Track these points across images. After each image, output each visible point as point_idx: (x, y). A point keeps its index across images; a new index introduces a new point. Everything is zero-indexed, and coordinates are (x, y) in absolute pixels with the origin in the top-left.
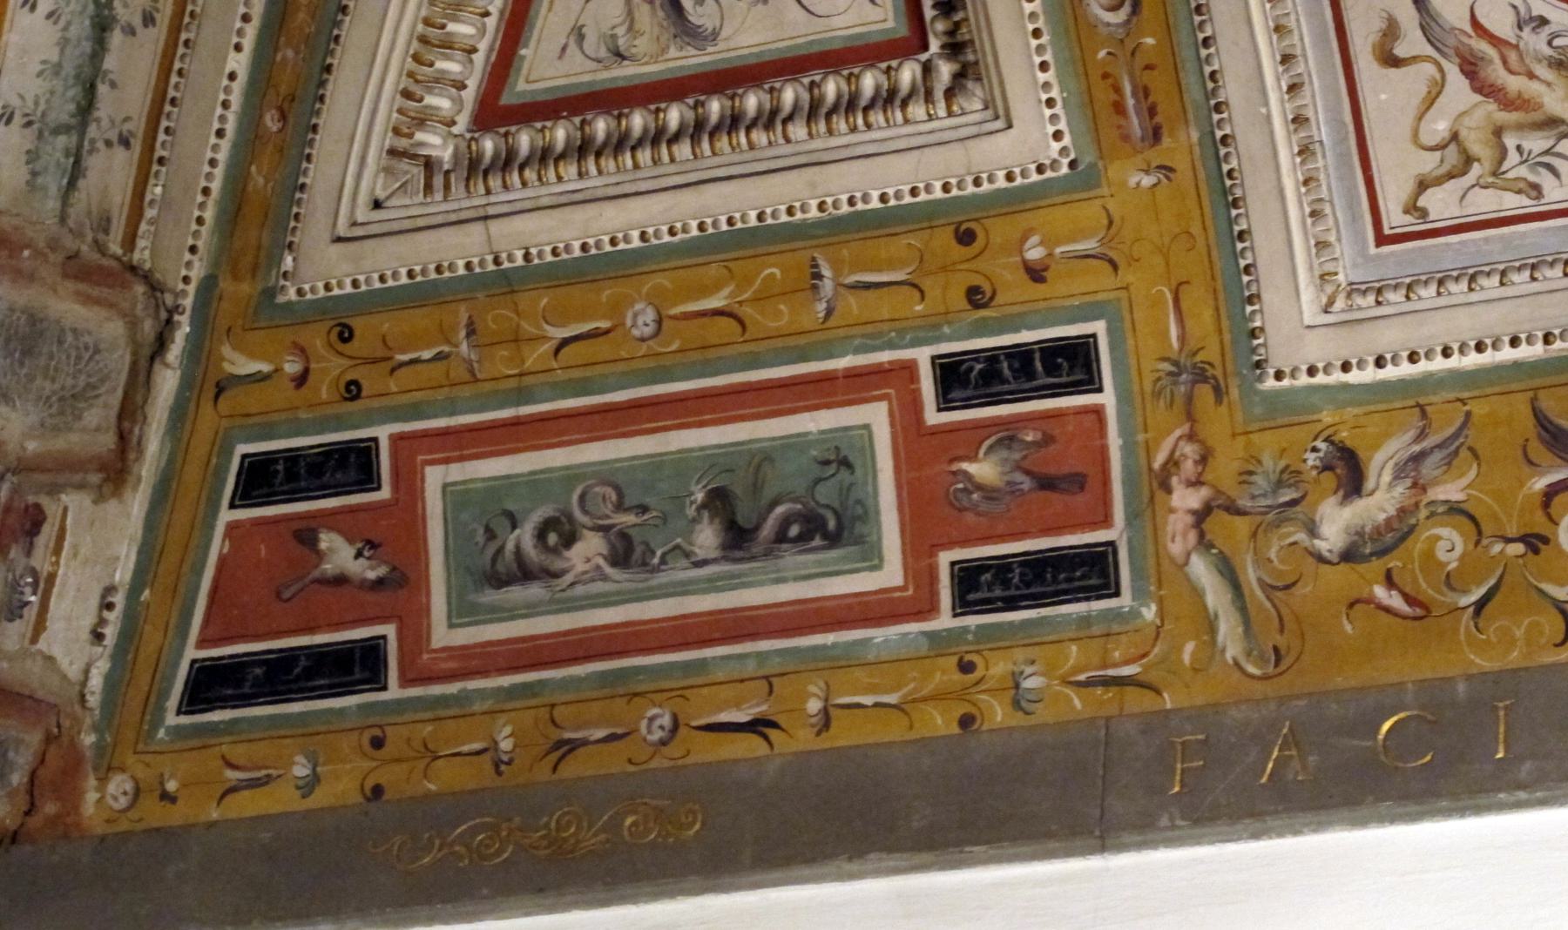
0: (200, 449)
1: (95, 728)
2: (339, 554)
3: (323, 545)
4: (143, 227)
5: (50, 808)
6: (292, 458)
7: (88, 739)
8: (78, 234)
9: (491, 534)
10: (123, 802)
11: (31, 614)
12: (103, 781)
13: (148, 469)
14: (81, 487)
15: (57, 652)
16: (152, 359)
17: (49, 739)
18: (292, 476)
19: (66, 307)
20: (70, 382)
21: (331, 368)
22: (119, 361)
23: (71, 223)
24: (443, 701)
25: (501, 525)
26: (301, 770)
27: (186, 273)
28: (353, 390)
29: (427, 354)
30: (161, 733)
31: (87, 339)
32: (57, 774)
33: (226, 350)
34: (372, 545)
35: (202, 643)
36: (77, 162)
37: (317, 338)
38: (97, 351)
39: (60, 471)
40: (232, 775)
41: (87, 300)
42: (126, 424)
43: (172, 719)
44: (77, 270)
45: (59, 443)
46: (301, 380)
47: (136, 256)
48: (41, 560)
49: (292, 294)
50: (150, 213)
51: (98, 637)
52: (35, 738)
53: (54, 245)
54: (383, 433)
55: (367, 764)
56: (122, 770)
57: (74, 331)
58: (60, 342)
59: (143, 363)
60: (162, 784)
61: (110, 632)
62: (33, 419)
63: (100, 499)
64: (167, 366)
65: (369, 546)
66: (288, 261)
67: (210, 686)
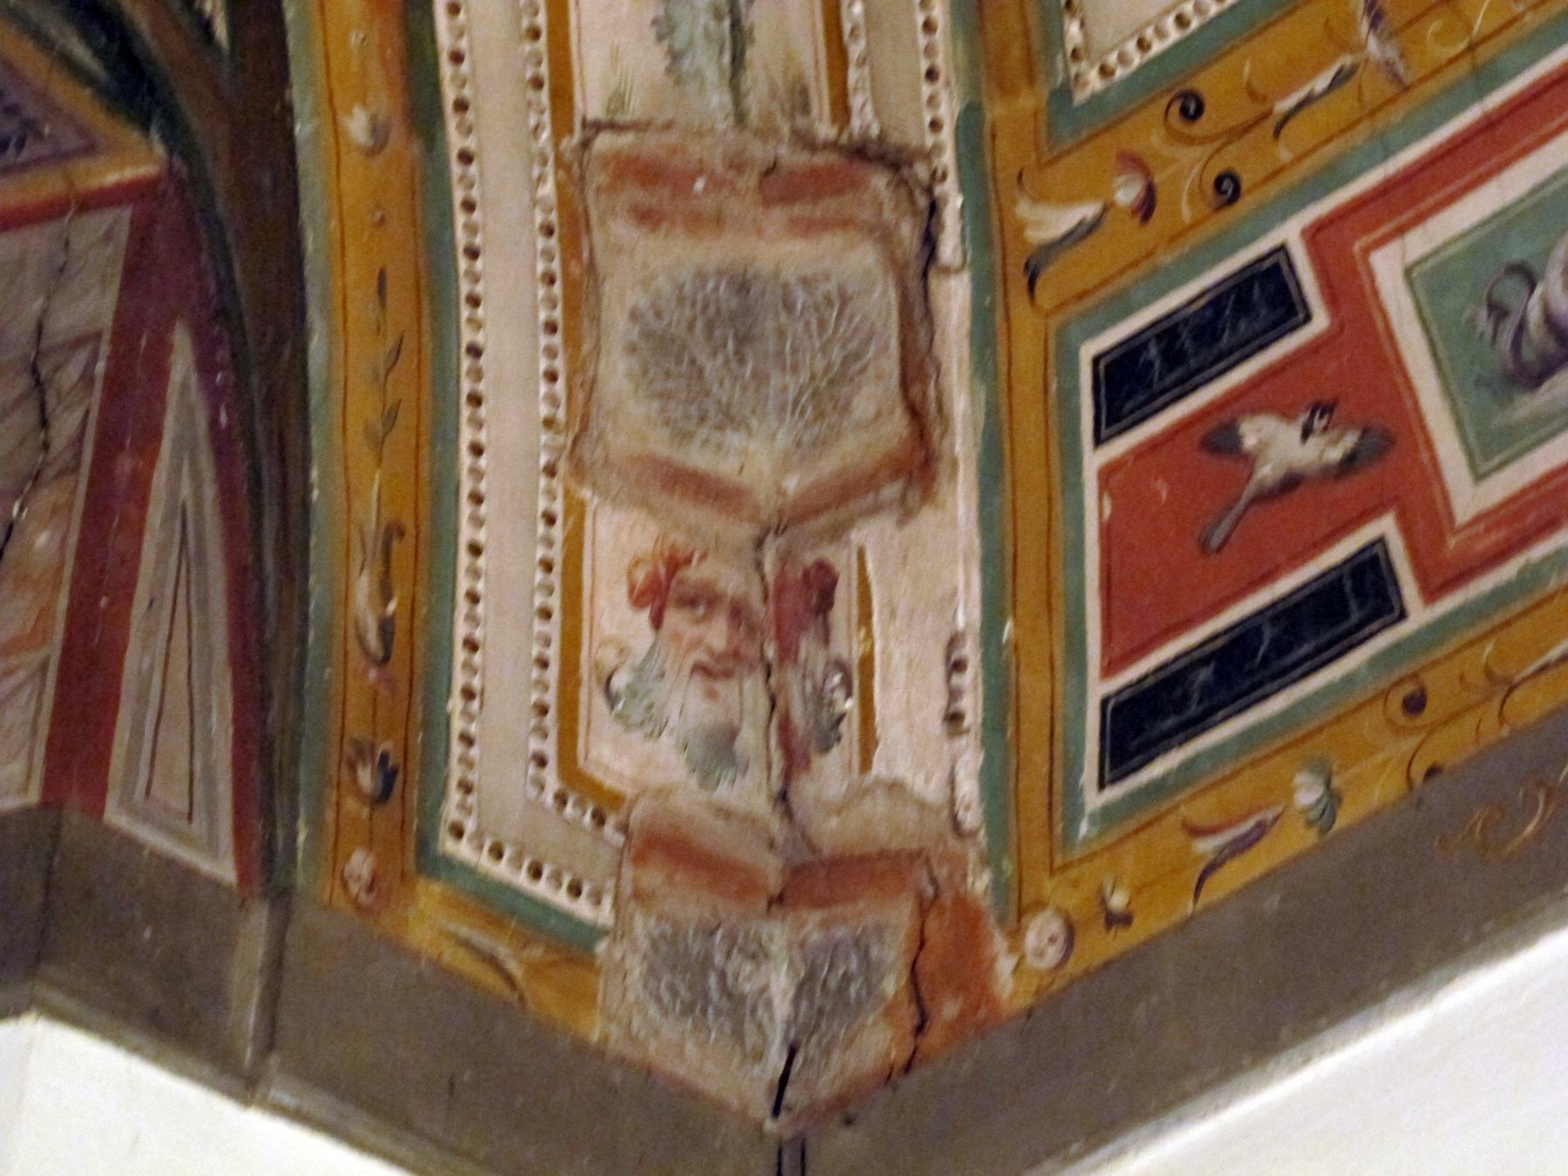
0: (1027, 387)
1: (987, 860)
2: (1278, 445)
3: (1250, 441)
4: (853, 75)
5: (949, 1009)
6: (1166, 331)
7: (980, 883)
8: (767, 133)
9: (1498, 311)
10: (1053, 954)
11: (850, 730)
12: (1016, 935)
13: (962, 443)
14: (876, 510)
15: (903, 770)
16: (925, 275)
17: (924, 908)
18: (1173, 357)
19: (783, 252)
20: (820, 365)
21: (1186, 168)
22: (880, 303)
23: (754, 117)
24: (1500, 596)
25: (1510, 290)
26: (1307, 793)
27: (932, 114)
28: (1227, 188)
29: (1321, 83)
30: (1084, 828)
31: (831, 287)
32: (947, 954)
33: (1024, 209)
34: (1324, 408)
35: (1109, 669)
36: (736, 25)
37: (1150, 133)
38: (845, 300)
39: (844, 498)
40: (1206, 846)
41: (808, 228)
42: (915, 391)
43: (1094, 800)
44: (779, 188)
45: (830, 464)
46: (1146, 207)
47: (856, 123)
48: (845, 644)
49: (1094, 82)
50: (856, 50)
51: (953, 719)
52: (900, 915)
53: (737, 164)
54: (1290, 232)
55: (1408, 744)
56: (1039, 905)
57: (805, 282)
58: (788, 306)
59: (914, 285)
60: (1103, 902)
61: (972, 706)
62: (783, 439)
63: (906, 515)
64: (946, 271)
65: (1321, 412)
66: (1073, 30)
67: (1136, 728)
